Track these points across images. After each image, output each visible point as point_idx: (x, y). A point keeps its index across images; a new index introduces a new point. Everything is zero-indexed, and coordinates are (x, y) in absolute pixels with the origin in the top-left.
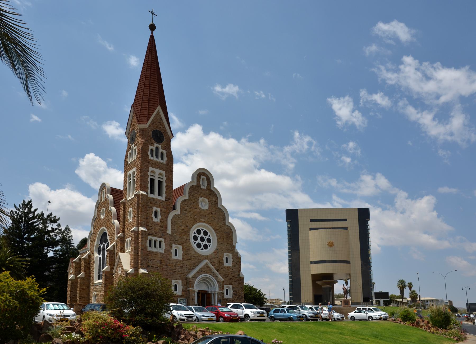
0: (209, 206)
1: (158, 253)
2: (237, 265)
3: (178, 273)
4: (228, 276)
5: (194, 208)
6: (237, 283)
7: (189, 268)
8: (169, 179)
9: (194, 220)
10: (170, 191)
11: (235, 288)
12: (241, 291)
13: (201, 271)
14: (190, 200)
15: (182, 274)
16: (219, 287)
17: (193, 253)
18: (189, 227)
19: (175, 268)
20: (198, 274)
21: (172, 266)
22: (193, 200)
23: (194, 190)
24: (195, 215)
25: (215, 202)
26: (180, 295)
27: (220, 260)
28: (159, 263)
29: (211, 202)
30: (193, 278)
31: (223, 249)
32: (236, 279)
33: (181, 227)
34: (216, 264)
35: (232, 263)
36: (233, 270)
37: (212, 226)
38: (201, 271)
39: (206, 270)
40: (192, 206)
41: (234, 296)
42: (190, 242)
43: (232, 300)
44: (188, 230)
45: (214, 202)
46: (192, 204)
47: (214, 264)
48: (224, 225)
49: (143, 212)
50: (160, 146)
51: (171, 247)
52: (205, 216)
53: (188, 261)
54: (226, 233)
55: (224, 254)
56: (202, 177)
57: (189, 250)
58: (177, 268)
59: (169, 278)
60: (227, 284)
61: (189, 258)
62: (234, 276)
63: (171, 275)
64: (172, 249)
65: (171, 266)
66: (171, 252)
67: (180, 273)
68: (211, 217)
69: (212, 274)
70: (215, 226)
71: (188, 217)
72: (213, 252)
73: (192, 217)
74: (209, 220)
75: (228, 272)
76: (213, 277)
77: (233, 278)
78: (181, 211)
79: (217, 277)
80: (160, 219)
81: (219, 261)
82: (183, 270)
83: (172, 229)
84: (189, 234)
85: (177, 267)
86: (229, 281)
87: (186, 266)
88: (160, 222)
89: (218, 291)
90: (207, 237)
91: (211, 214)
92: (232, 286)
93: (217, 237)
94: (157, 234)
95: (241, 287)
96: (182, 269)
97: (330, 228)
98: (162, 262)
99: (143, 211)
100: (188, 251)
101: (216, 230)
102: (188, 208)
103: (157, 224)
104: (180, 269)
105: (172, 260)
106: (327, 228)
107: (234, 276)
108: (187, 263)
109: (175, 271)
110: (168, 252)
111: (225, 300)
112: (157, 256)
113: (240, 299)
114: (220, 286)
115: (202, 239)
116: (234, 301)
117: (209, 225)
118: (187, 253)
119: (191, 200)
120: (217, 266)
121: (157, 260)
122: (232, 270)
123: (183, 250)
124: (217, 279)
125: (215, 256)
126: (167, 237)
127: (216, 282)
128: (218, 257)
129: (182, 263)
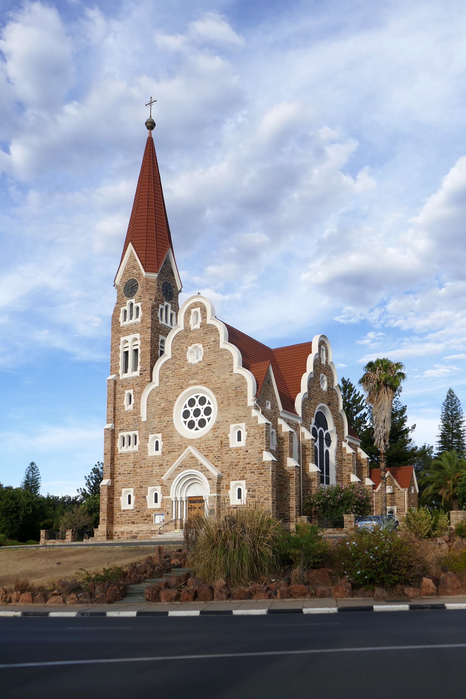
2: (255, 441)
3: (156, 476)
4: (237, 465)
5: (180, 368)
8: (145, 341)
9: (179, 387)
11: (252, 485)
12: (265, 487)
13: (183, 466)
16: (211, 488)
17: (176, 440)
19: (153, 469)
20: (177, 472)
21: (148, 466)
23: (180, 340)
25: (215, 341)
28: (132, 466)
29: (207, 346)
30: (169, 479)
31: (228, 420)
32: (253, 467)
33: (160, 405)
34: (216, 449)
35: (247, 440)
37: (209, 385)
38: (181, 467)
39: (189, 464)
40: (177, 366)
41: (249, 500)
42: (173, 423)
44: (170, 406)
45: (212, 343)
47: (211, 449)
50: (133, 301)
51: (147, 440)
52: (197, 373)
54: (233, 389)
55: (229, 428)
57: (171, 437)
58: (155, 468)
59: (143, 486)
60: (236, 480)
61: (171, 449)
62: (249, 463)
63: (147, 480)
64: (148, 442)
66: (147, 447)
68: (208, 370)
69: (199, 467)
70: (214, 384)
71: (171, 386)
73: (176, 384)
74: (204, 377)
75: (239, 457)
76: (201, 471)
78: (160, 380)
79: (208, 470)
80: (133, 404)
82: (163, 470)
83: (148, 413)
84: (172, 413)
85: (155, 466)
86: (240, 473)
87: (166, 463)
91: (208, 365)
92: (246, 482)
94: (129, 427)
95: (264, 481)
100: (170, 439)
101: (215, 390)
102: (170, 372)
103: (129, 413)
104: (159, 469)
107: (249, 463)
109: (152, 474)
110: (144, 449)
111: (232, 509)
112: (129, 457)
114: (213, 485)
117: (203, 386)
118: (169, 442)
119: (176, 358)
120: (217, 452)
121: (129, 463)
122: (245, 453)
123: (163, 439)
127: (207, 480)
128: (218, 435)
129: (161, 460)
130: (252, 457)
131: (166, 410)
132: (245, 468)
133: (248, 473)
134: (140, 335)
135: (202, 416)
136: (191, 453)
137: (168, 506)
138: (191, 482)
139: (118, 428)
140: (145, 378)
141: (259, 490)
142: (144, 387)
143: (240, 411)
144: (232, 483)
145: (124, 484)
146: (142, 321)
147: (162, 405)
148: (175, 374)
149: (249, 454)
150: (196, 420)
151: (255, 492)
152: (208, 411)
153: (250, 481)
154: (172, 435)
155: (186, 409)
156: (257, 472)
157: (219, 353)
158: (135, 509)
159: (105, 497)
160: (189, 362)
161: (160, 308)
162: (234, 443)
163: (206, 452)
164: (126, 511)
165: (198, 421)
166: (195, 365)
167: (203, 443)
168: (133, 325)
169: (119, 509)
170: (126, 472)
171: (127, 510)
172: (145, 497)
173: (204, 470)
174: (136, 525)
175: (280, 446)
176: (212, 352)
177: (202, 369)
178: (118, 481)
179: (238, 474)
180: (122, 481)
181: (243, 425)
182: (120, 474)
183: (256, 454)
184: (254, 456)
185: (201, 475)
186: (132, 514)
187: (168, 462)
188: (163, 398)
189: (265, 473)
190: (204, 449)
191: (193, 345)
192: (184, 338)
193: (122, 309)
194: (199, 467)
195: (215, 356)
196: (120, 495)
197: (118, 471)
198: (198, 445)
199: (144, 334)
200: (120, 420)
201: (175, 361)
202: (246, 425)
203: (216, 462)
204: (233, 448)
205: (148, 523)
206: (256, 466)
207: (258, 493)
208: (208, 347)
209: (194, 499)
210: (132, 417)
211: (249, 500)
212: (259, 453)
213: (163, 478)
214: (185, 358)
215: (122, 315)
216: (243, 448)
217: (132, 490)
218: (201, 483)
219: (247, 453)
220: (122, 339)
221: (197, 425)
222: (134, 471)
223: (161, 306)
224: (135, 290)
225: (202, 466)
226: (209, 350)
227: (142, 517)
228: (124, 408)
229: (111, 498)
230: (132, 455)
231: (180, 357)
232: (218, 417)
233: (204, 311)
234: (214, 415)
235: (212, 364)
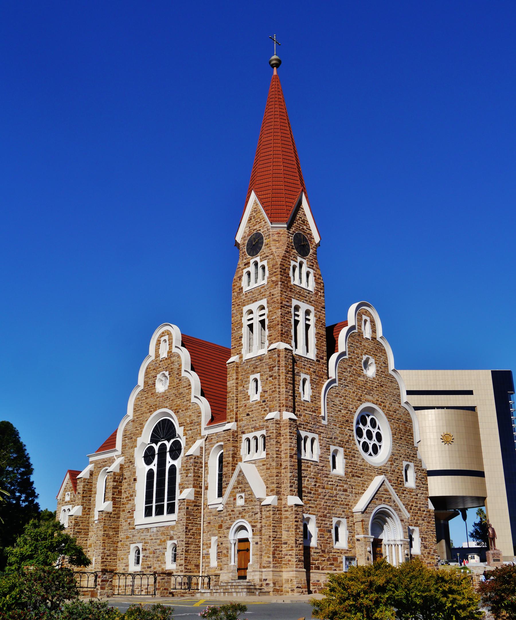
10: (322, 344)
22: (355, 361)
25: (385, 363)
28: (313, 483)
35: (416, 483)
36: (417, 495)
46: (354, 367)
48: (399, 407)
63: (330, 508)
72: (387, 460)
80: (311, 396)
84: (352, 426)
85: (340, 490)
88: (311, 401)
89: (402, 538)
90: (376, 430)
94: (307, 425)
97: (442, 408)
98: (316, 482)
103: (306, 407)
104: (343, 494)
105: (331, 478)
106: (438, 408)
112: (309, 469)
115: (369, 435)
118: (352, 463)
126: (323, 431)
127: (399, 521)
147: (342, 411)
158: (319, 547)
173: (397, 509)
174: (320, 571)
181: (412, 465)
188: (342, 404)
191: (367, 356)
205: (335, 570)
206: (425, 513)
210: (310, 413)
222: (316, 491)
227: (328, 560)
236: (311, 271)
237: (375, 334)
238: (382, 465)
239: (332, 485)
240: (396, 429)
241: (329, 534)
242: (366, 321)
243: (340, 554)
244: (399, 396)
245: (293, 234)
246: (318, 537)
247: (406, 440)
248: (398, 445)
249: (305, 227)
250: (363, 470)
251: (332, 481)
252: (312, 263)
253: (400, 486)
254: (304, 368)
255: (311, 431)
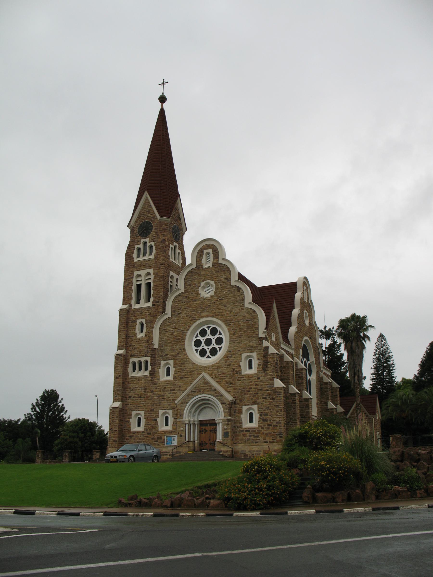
0: (216, 290)
1: (142, 378)
3: (167, 400)
4: (249, 391)
5: (193, 301)
6: (268, 400)
7: (183, 390)
9: (191, 319)
10: (159, 291)
11: (264, 409)
12: (277, 411)
14: (186, 293)
15: (172, 400)
16: (224, 412)
17: (189, 366)
18: (184, 331)
23: (192, 276)
24: (194, 311)
25: (227, 279)
26: (170, 431)
27: (233, 368)
29: (219, 283)
30: (182, 403)
31: (240, 349)
32: (265, 393)
33: (172, 334)
38: (195, 392)
39: (202, 389)
40: (190, 300)
41: (261, 423)
42: (185, 351)
43: (258, 431)
44: (183, 335)
45: (224, 281)
46: (190, 296)
47: (223, 376)
49: (122, 331)
52: (209, 306)
53: (182, 379)
54: (245, 322)
55: (241, 357)
56: (205, 251)
57: (184, 364)
58: (166, 392)
60: (248, 405)
61: (183, 375)
63: (158, 404)
65: (158, 392)
67: (170, 400)
70: (226, 317)
71: (183, 317)
72: (222, 357)
73: (188, 316)
74: (216, 310)
75: (251, 383)
76: (215, 397)
77: (259, 392)
78: (173, 311)
79: (222, 395)
80: (145, 333)
81: (233, 369)
84: (184, 341)
85: (166, 391)
88: (145, 336)
91: (220, 300)
92: (258, 407)
93: (229, 332)
94: (141, 353)
96: (173, 393)
99: (123, 329)
100: (182, 365)
101: (227, 322)
102: (182, 304)
104: (170, 393)
105: (160, 384)
107: (261, 390)
108: (180, 382)
109: (163, 398)
111: (244, 432)
112: (140, 382)
113: (274, 426)
115: (208, 342)
116: (261, 431)
118: (181, 369)
120: (229, 379)
121: (140, 387)
122: (257, 380)
124: (222, 400)
125: (226, 362)
127: (220, 405)
128: (230, 363)
129: (173, 385)
130: (264, 384)
131: (178, 339)
132: (258, 393)
133: (260, 398)
134: (153, 270)
135: (214, 345)
136: (205, 379)
137: (182, 429)
138: (203, 407)
139: (130, 354)
140: (157, 309)
141: (271, 414)
142: (156, 317)
143: (252, 342)
144: (245, 408)
145: (134, 407)
146: (156, 258)
148: (187, 307)
149: (260, 381)
150: (208, 349)
151: (267, 416)
152: (219, 341)
153: (262, 406)
154: (184, 362)
155: (197, 338)
156: (269, 397)
157: (230, 289)
158: (145, 431)
159: (116, 419)
160: (201, 296)
161: (171, 248)
162: (246, 371)
163: (218, 378)
164: (136, 433)
165: (209, 350)
166: (208, 299)
167: (215, 370)
168: (147, 261)
169: (128, 431)
170: (137, 396)
171: (138, 432)
172: (156, 420)
173: (218, 395)
175: (282, 375)
176: (224, 288)
177: (214, 303)
178: (128, 404)
179: (250, 399)
180: (132, 404)
181: (254, 354)
182: (130, 397)
183: (267, 381)
184: (266, 383)
185: (216, 400)
186: (142, 436)
187: (180, 387)
188: (175, 328)
189: (276, 399)
190: (216, 376)
191: (205, 281)
192: (196, 275)
193: (136, 247)
194: (213, 393)
195: (227, 292)
196: (130, 418)
197: (128, 395)
198: (210, 372)
199: (157, 270)
200: (132, 347)
201: (188, 294)
202: (257, 354)
203: (229, 388)
204: (245, 375)
205: (159, 445)
206: (268, 392)
207: (270, 417)
208: (220, 283)
209: (205, 422)
210: (143, 344)
211: (261, 423)
212: (271, 380)
213: (176, 402)
214: (197, 292)
215: (135, 252)
216: (255, 376)
217: (142, 413)
218: (213, 408)
219: (258, 380)
220: (136, 273)
221: (208, 353)
222: (145, 395)
223: (171, 246)
224: (149, 231)
225: (216, 391)
226: (221, 286)
227: (152, 439)
228: (136, 336)
229: (121, 420)
230: (143, 380)
231: (193, 291)
232: (230, 347)
233: (216, 252)
234: (225, 345)
235: (223, 298)
236: (153, 244)
237: (217, 259)
238: (215, 363)
239: (160, 388)
240: (236, 330)
241: (154, 422)
242: (208, 253)
243: (164, 434)
244: (243, 300)
245: (138, 226)
246: (145, 425)
247: (247, 335)
248: (236, 342)
249: (149, 215)
250: (193, 372)
251: (161, 386)
252: (154, 236)
253: (237, 375)
254: (141, 315)
255: (143, 356)
